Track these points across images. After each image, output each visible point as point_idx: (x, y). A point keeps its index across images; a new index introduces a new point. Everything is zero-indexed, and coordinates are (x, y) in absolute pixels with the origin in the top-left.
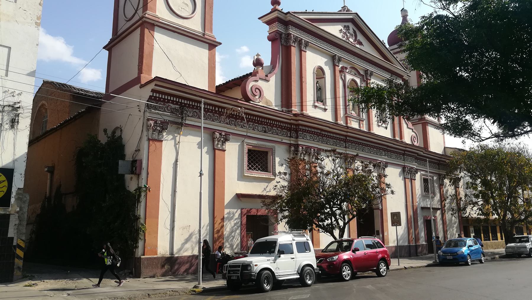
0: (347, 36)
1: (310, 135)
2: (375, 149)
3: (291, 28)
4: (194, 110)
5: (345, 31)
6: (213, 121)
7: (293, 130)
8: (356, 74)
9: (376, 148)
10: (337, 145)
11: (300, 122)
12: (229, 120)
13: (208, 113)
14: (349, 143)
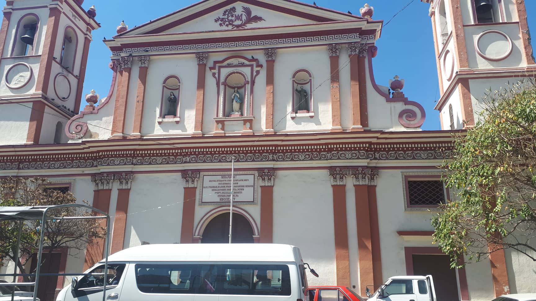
0: (229, 21)
1: (121, 158)
2: (248, 155)
3: (124, 51)
6: (5, 169)
7: (98, 159)
9: (249, 153)
10: (170, 163)
11: (90, 148)
12: (22, 165)
14: (193, 156)
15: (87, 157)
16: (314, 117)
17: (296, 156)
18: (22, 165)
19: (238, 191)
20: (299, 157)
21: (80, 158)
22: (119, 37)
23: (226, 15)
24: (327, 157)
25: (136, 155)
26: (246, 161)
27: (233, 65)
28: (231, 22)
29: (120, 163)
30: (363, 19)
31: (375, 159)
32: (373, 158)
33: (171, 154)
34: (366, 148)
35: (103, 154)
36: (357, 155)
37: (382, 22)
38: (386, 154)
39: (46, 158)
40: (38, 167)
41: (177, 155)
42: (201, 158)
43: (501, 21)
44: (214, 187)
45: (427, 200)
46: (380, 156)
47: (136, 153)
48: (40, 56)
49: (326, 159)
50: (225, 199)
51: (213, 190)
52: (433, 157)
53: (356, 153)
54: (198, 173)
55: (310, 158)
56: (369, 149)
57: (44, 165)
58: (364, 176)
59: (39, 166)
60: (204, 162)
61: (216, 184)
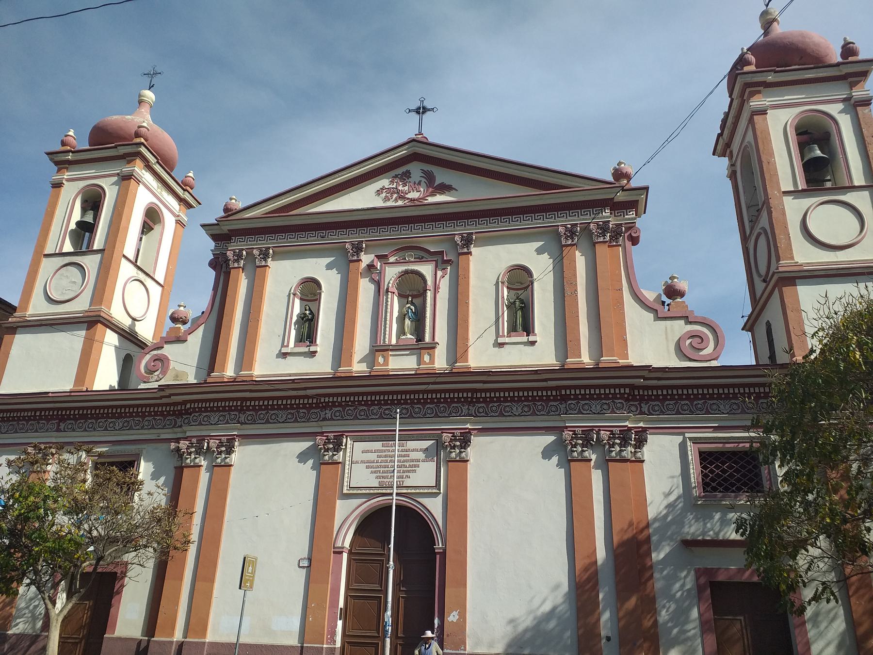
1: (221, 413)
4: (10, 423)
5: (394, 186)
6: (36, 431)
8: (423, 257)
11: (172, 397)
12: (64, 424)
13: (30, 422)
14: (336, 409)
15: (166, 411)
16: (536, 344)
17: (508, 409)
18: (64, 424)
19: (410, 469)
20: (512, 410)
21: (156, 414)
22: (227, 219)
23: (395, 184)
24: (560, 411)
25: (245, 408)
26: (424, 416)
27: (405, 261)
28: (402, 194)
29: (218, 421)
30: (615, 184)
31: (642, 413)
32: (638, 411)
33: (301, 406)
34: (626, 396)
35: (192, 406)
36: (611, 407)
37: (646, 189)
38: (660, 405)
39: (102, 413)
40: (88, 428)
41: (311, 406)
42: (350, 412)
43: (848, 185)
44: (368, 462)
45: (733, 485)
46: (650, 409)
47: (244, 405)
48: (105, 249)
49: (557, 413)
50: (387, 483)
51: (367, 467)
52: (740, 410)
53: (608, 404)
54: (345, 436)
55: (531, 412)
56: (630, 398)
57: (97, 424)
58: (623, 443)
59: (90, 426)
60: (356, 418)
61: (373, 456)
